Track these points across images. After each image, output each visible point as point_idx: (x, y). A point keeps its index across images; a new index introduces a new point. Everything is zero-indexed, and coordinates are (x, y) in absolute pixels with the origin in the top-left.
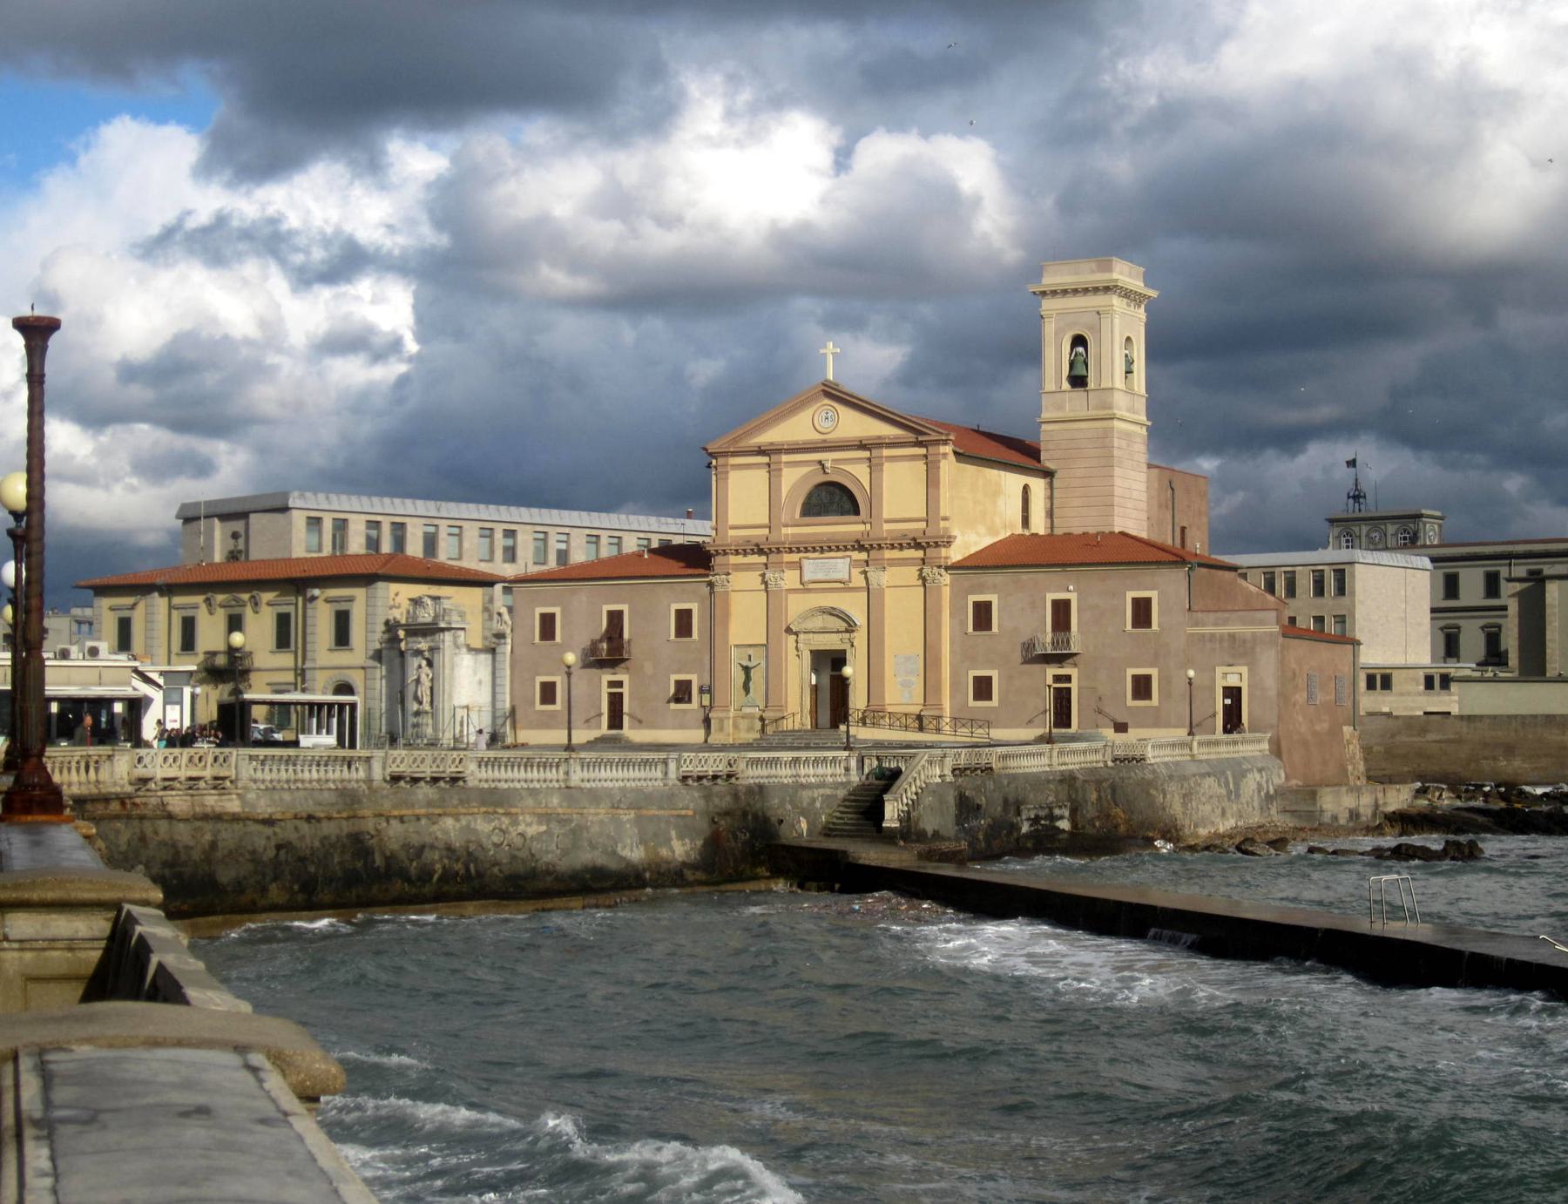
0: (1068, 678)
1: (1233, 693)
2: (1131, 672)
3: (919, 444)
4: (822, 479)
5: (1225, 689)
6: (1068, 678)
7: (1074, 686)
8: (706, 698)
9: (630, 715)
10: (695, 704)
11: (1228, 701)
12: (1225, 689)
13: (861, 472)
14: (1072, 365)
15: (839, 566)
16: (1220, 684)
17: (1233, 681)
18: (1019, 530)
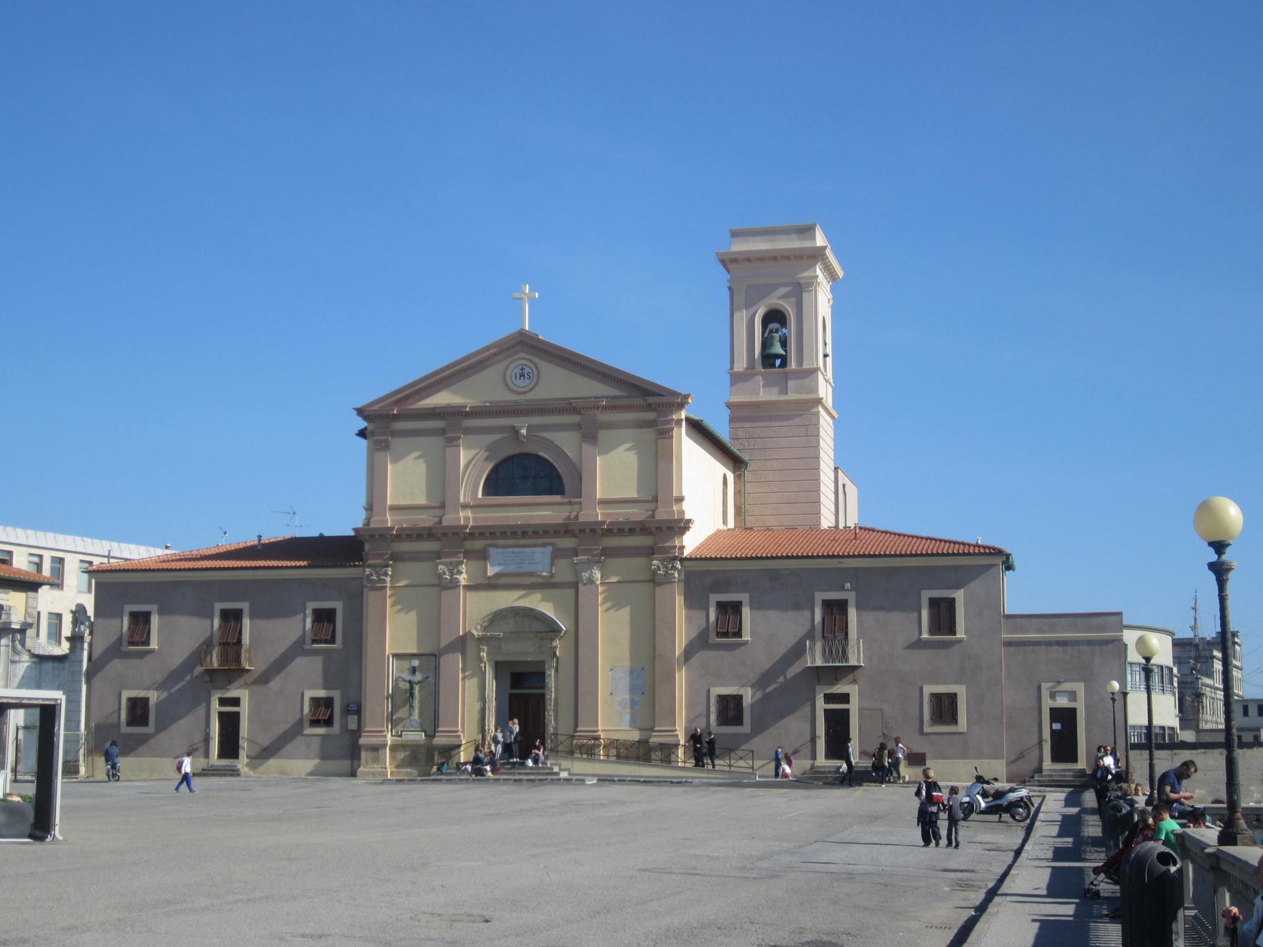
0: (845, 698)
1: (1066, 717)
2: (929, 689)
3: (650, 407)
4: (512, 450)
5: (1053, 710)
6: (845, 698)
7: (853, 707)
8: (352, 723)
9: (248, 740)
10: (336, 728)
11: (1057, 726)
12: (1053, 710)
13: (566, 442)
14: (766, 344)
15: (538, 559)
16: (1047, 704)
17: (1062, 702)
18: (722, 527)
